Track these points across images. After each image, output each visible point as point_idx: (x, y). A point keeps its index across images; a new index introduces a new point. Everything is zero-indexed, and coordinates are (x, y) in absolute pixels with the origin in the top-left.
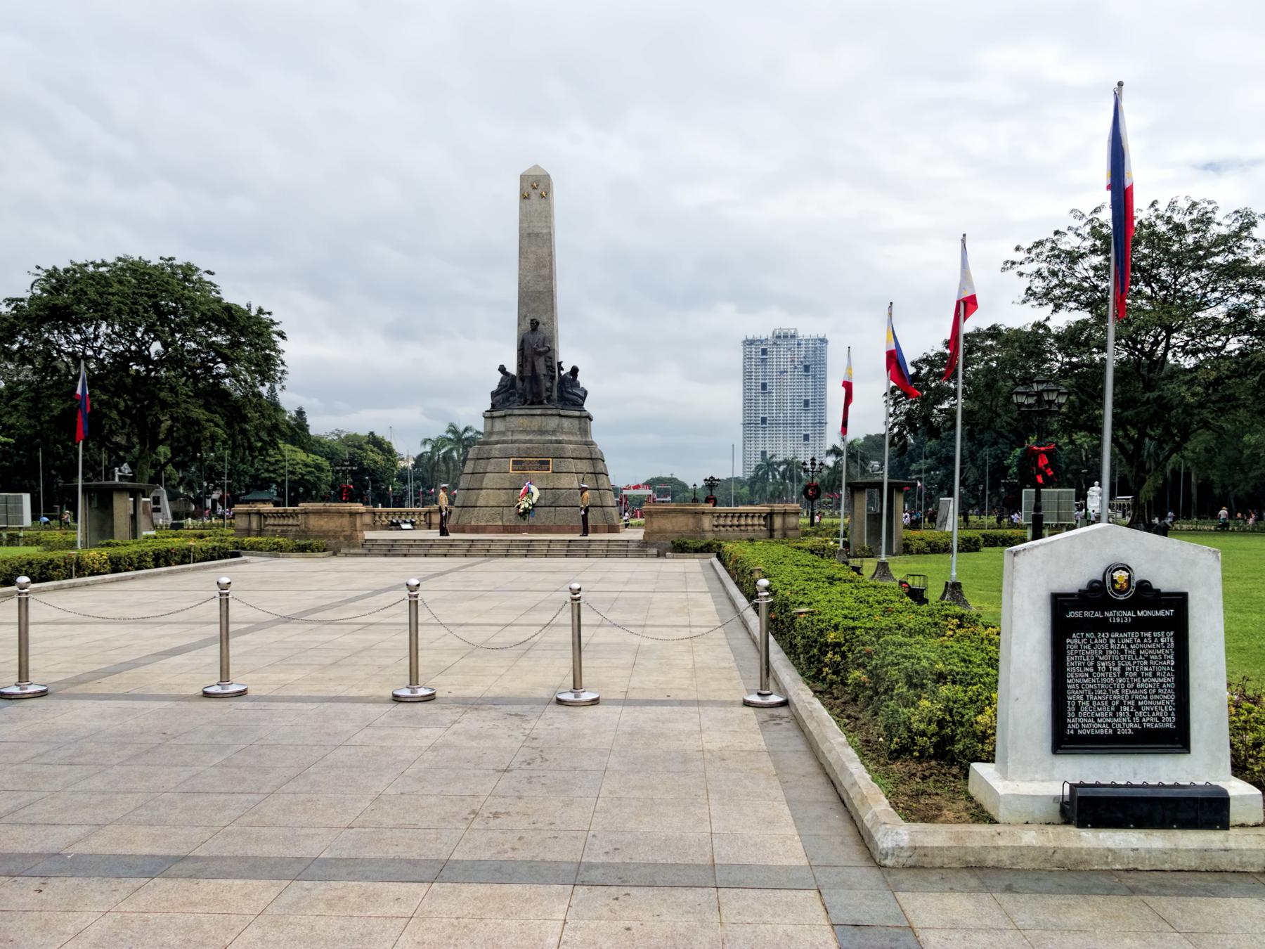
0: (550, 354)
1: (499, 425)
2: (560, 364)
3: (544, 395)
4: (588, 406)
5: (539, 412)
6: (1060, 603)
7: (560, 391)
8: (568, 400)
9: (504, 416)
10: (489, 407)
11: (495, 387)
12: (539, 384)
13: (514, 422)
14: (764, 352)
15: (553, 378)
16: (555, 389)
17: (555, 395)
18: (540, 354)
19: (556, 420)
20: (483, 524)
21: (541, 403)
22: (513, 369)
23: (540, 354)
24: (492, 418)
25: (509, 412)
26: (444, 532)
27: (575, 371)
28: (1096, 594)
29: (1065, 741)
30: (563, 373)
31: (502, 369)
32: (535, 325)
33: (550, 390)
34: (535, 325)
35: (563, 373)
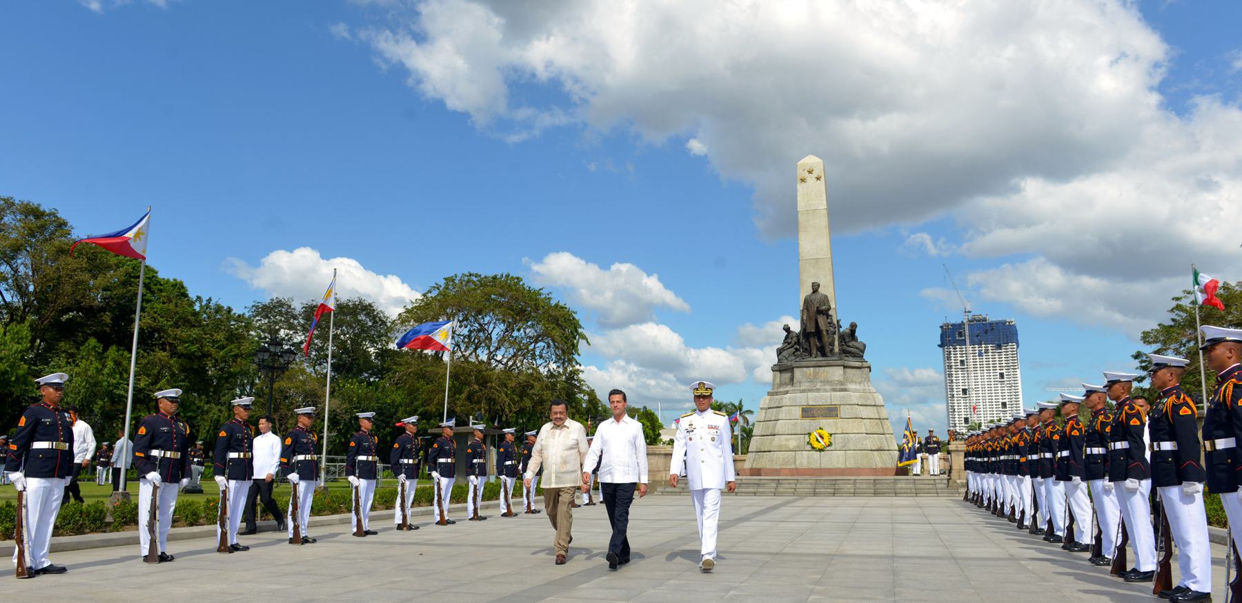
5: (824, 363)
8: (849, 352)
10: (776, 361)
16: (836, 343)
17: (837, 349)
19: (840, 370)
22: (796, 327)
27: (853, 328)
33: (832, 344)
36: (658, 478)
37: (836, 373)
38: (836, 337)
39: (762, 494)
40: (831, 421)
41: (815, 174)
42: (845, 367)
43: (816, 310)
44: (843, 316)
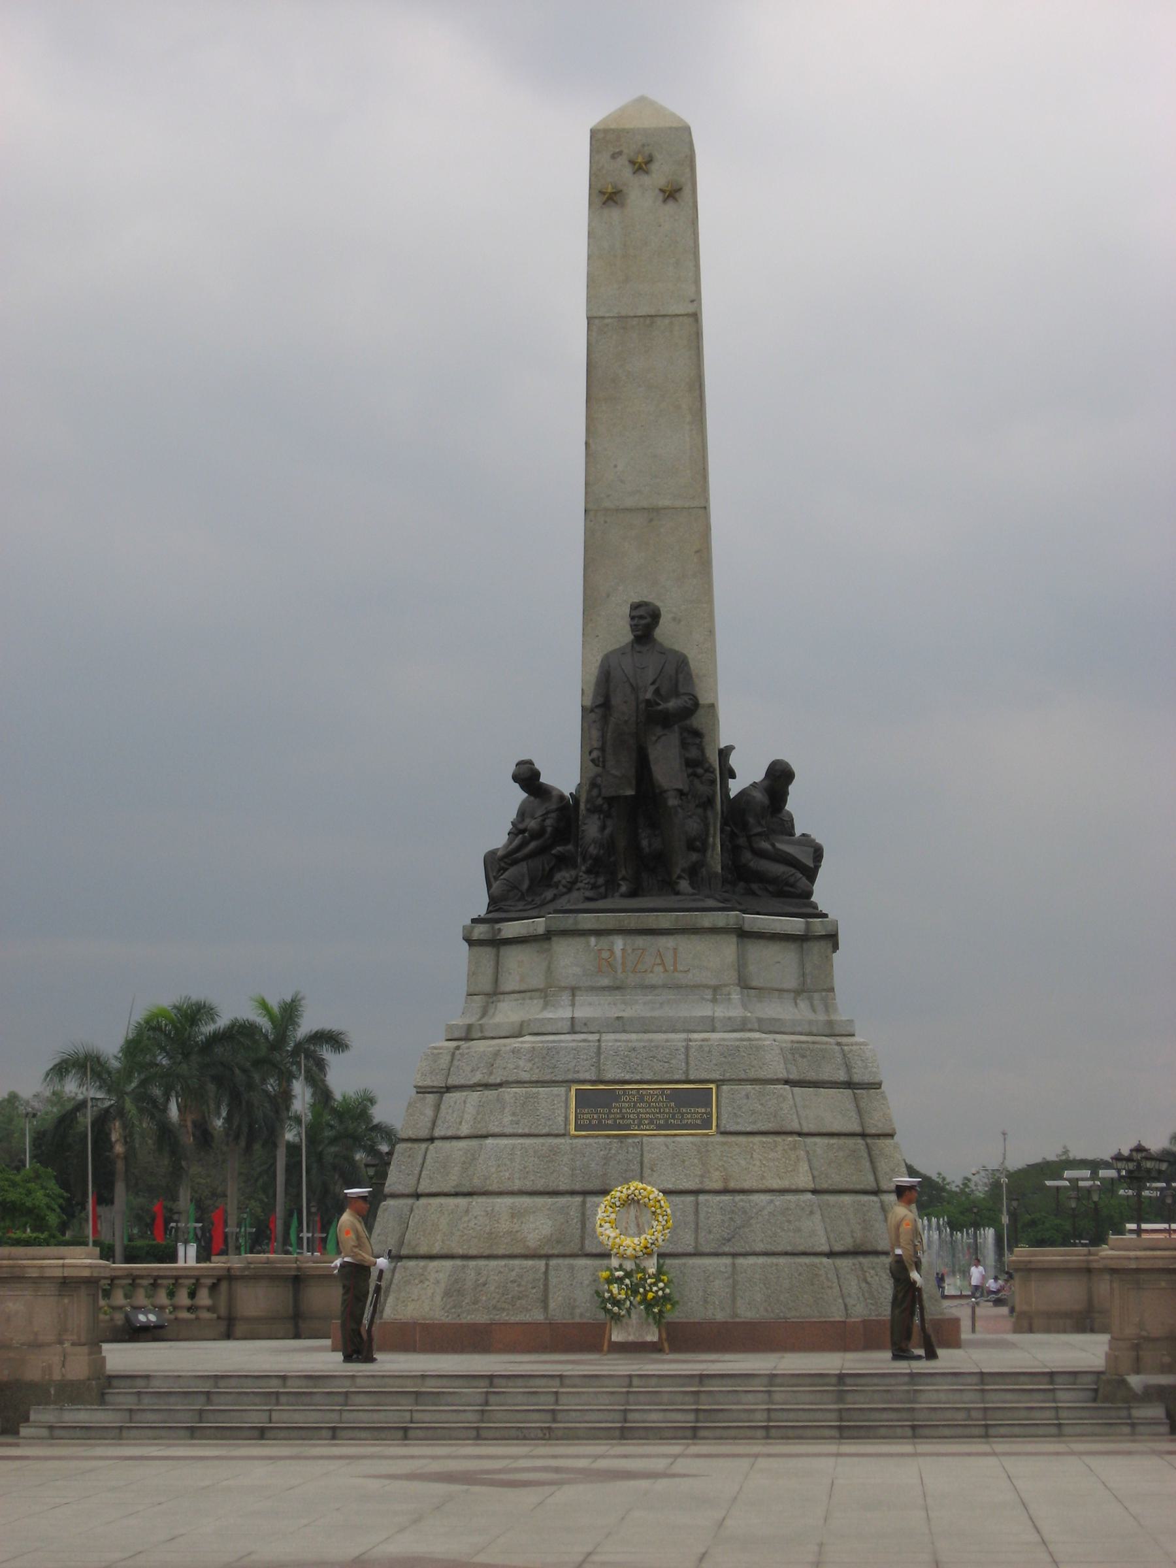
0: (697, 721)
1: (520, 965)
2: (725, 753)
3: (682, 861)
7: (732, 850)
8: (761, 877)
9: (548, 936)
10: (481, 909)
11: (499, 839)
12: (652, 823)
15: (709, 802)
16: (716, 841)
17: (716, 859)
18: (666, 720)
19: (728, 948)
20: (482, 1318)
21: (669, 886)
22: (564, 774)
23: (666, 720)
24: (497, 943)
25: (568, 921)
26: (357, 1348)
27: (779, 777)
30: (735, 787)
31: (527, 777)
32: (645, 621)
33: (697, 844)
34: (645, 621)
36: (33, 1373)
37: (712, 957)
39: (434, 1434)
40: (686, 1140)
41: (660, 175)
42: (743, 934)
43: (648, 702)
44: (747, 741)
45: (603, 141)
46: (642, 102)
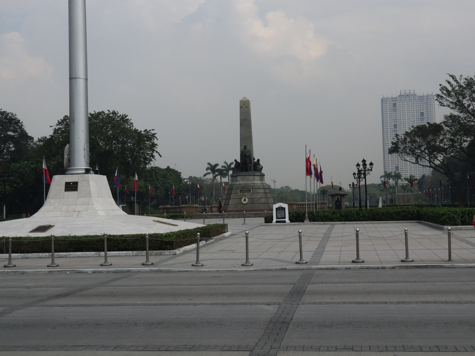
4: (263, 171)
6: (276, 208)
7: (254, 167)
13: (239, 178)
14: (395, 105)
17: (252, 168)
18: (247, 156)
19: (253, 177)
21: (248, 171)
22: (239, 160)
27: (258, 160)
28: (279, 208)
29: (277, 218)
31: (236, 161)
32: (245, 147)
33: (251, 167)
34: (245, 147)
35: (255, 161)
38: (252, 164)
42: (254, 175)
45: (241, 102)
46: (245, 97)
